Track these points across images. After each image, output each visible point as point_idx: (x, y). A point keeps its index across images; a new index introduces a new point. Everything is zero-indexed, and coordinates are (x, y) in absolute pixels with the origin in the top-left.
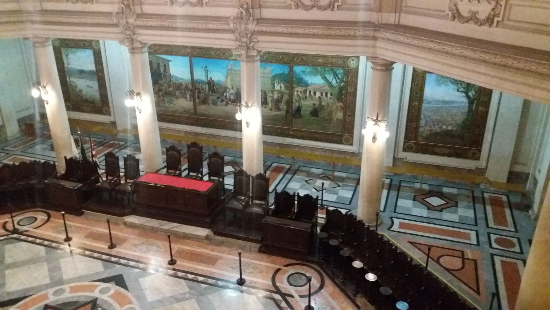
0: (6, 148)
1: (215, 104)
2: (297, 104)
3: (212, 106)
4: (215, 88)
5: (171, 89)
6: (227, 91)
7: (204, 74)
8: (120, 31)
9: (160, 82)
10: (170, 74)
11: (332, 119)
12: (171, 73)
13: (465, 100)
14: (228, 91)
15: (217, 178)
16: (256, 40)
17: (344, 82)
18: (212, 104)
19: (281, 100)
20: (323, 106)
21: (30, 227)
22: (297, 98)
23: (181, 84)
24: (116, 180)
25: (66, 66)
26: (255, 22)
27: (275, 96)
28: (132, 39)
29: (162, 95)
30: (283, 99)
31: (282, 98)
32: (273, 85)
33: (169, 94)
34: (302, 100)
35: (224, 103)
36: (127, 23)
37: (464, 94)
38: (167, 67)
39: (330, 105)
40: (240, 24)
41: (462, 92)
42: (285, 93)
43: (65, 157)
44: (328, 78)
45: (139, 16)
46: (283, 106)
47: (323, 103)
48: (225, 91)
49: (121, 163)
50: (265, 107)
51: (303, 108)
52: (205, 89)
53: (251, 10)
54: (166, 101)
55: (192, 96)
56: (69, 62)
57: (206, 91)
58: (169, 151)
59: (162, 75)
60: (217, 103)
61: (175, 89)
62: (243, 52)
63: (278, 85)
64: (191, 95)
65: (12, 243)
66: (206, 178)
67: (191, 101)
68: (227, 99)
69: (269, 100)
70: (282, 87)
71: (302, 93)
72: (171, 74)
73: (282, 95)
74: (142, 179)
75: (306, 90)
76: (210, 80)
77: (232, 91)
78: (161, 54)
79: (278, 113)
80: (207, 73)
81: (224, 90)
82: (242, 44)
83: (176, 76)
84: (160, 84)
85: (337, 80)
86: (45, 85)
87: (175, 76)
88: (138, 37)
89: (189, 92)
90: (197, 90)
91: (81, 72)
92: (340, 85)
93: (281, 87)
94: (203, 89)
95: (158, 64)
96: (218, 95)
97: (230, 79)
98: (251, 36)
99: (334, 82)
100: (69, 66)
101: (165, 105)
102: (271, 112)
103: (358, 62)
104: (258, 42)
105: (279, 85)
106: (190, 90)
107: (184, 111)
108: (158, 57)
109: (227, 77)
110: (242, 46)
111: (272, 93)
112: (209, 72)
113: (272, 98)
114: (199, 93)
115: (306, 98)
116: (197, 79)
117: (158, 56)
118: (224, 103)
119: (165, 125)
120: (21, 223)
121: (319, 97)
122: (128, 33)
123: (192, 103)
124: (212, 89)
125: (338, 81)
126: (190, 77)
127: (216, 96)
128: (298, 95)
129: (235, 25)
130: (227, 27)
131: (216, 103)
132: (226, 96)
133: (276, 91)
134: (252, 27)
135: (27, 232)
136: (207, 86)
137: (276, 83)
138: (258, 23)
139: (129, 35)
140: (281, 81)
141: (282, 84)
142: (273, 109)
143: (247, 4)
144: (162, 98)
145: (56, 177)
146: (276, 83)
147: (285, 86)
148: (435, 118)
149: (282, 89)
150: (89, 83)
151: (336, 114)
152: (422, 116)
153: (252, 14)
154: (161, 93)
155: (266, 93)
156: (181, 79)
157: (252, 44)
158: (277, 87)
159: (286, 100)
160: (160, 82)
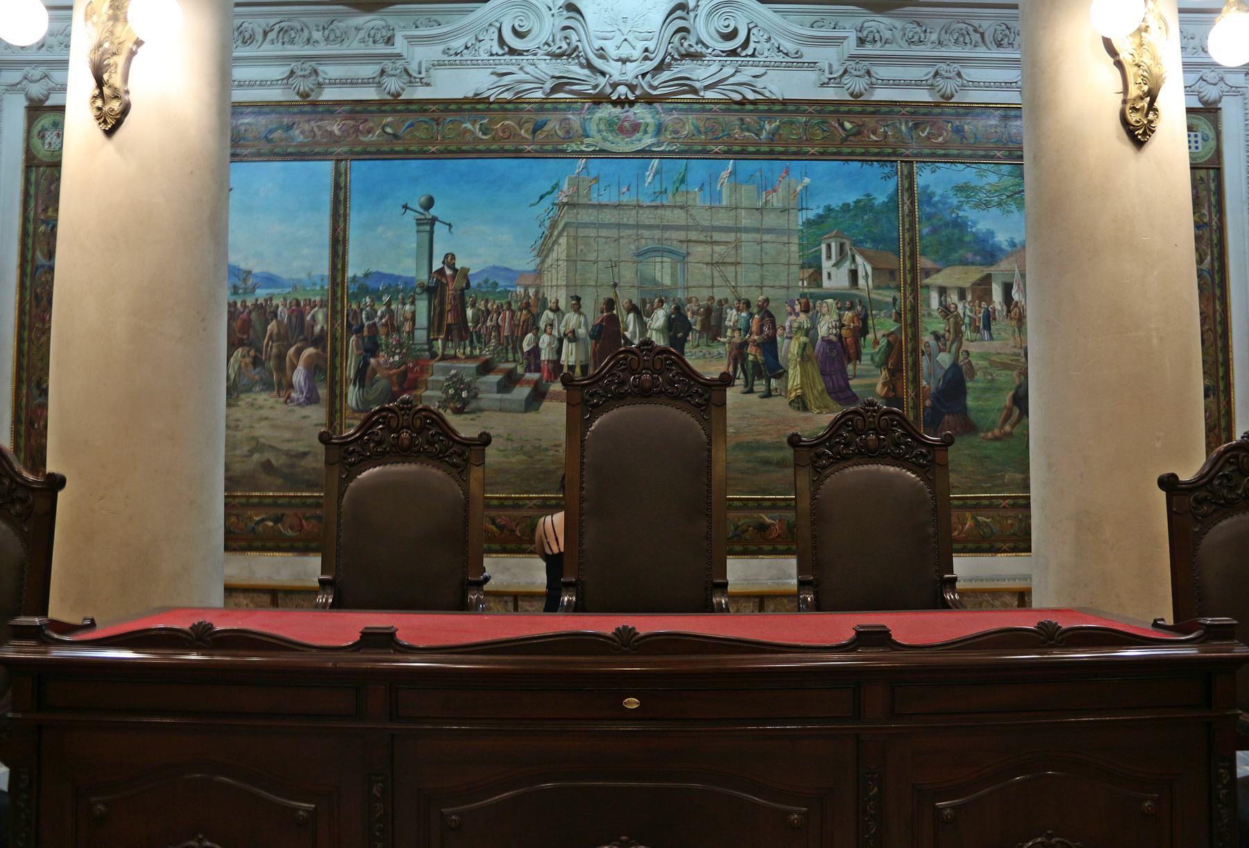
2: (945, 359)
4: (469, 312)
6: (542, 325)
7: (411, 240)
19: (857, 343)
22: (940, 326)
23: (266, 311)
27: (823, 330)
30: (870, 336)
31: (863, 331)
34: (968, 334)
35: (522, 392)
42: (880, 305)
48: (532, 325)
50: (768, 394)
51: (979, 375)
52: (407, 327)
57: (411, 333)
60: (475, 397)
64: (314, 369)
67: (312, 399)
68: (538, 369)
69: (790, 348)
70: (861, 273)
71: (969, 298)
73: (864, 320)
75: (987, 280)
76: (441, 271)
77: (572, 319)
80: (431, 233)
81: (522, 316)
93: (854, 274)
94: (392, 327)
96: (487, 353)
97: (563, 256)
102: (803, 415)
103: (1212, 135)
105: (847, 265)
106: (318, 341)
107: (267, 466)
109: (544, 251)
111: (806, 310)
113: (804, 339)
114: (372, 349)
115: (989, 318)
116: (366, 275)
118: (522, 392)
123: (317, 415)
126: (324, 268)
127: (471, 357)
128: (946, 311)
131: (465, 402)
132: (536, 351)
136: (422, 306)
137: (829, 257)
140: (855, 243)
141: (859, 259)
142: (810, 399)
146: (829, 257)
149: (861, 282)
155: (770, 315)
156: (270, 280)
158: (836, 279)
159: (883, 342)
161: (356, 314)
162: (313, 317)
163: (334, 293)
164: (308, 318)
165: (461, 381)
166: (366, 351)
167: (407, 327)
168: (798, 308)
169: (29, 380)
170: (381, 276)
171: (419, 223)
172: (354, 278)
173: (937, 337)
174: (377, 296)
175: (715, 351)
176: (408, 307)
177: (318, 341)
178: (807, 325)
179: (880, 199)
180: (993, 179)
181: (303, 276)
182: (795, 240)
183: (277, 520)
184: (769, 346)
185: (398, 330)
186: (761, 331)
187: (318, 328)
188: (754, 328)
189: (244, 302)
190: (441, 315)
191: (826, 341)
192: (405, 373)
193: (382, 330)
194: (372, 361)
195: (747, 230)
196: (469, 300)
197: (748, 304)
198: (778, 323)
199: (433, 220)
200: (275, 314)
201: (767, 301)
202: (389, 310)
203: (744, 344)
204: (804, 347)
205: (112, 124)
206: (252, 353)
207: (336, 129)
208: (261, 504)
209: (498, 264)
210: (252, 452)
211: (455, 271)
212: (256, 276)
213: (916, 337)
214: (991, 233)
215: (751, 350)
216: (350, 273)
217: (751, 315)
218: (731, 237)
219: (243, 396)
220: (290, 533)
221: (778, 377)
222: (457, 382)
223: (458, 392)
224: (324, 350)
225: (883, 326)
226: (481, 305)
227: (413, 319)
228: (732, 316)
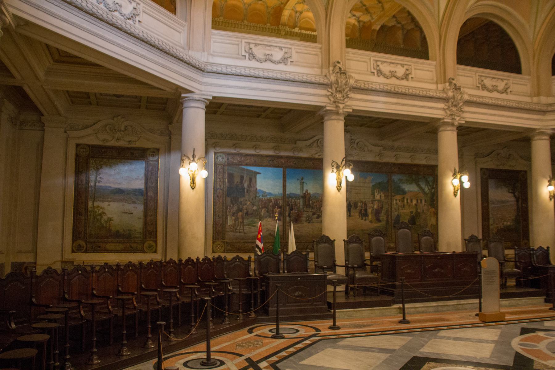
2: (396, 213)
3: (306, 224)
4: (311, 202)
5: (255, 208)
7: (299, 187)
9: (241, 200)
10: (257, 189)
11: (427, 225)
13: (513, 199)
17: (433, 188)
20: (419, 213)
22: (395, 207)
23: (269, 201)
25: (92, 184)
27: (375, 207)
30: (384, 209)
31: (382, 208)
32: (373, 194)
34: (400, 208)
37: (513, 194)
38: (253, 180)
39: (425, 212)
41: (511, 193)
44: (422, 186)
46: (383, 217)
47: (419, 210)
50: (365, 220)
52: (299, 205)
54: (245, 223)
56: (98, 179)
57: (299, 206)
60: (312, 220)
61: (261, 207)
63: (378, 194)
64: (280, 214)
69: (369, 211)
70: (382, 196)
73: (382, 205)
75: (404, 198)
76: (305, 193)
79: (379, 224)
80: (303, 185)
83: (264, 190)
84: (241, 203)
85: (429, 186)
87: (262, 191)
92: (431, 191)
94: (296, 205)
95: (242, 177)
96: (314, 211)
99: (426, 189)
100: (97, 184)
101: (244, 230)
102: (371, 224)
106: (281, 207)
108: (244, 170)
111: (372, 203)
112: (305, 185)
115: (404, 206)
116: (290, 193)
117: (243, 168)
121: (415, 204)
124: (307, 203)
125: (430, 188)
126: (281, 191)
127: (311, 211)
128: (397, 203)
131: (310, 221)
133: (377, 201)
136: (301, 201)
137: (376, 193)
141: (382, 193)
144: (240, 220)
147: (385, 196)
148: (499, 216)
149: (382, 198)
150: (129, 207)
151: (430, 220)
152: (491, 216)
154: (240, 213)
155: (366, 204)
156: (270, 194)
158: (377, 197)
161: (288, 202)
162: (279, 203)
163: (284, 197)
164: (278, 202)
165: (309, 216)
166: (291, 210)
167: (299, 205)
168: (371, 203)
169: (216, 215)
170: (293, 194)
171: (301, 183)
172: (288, 194)
173: (395, 209)
174: (292, 198)
175: (356, 211)
176: (299, 201)
177: (281, 207)
178: (372, 206)
179: (385, 181)
180: (405, 178)
181: (277, 193)
182: (370, 189)
185: (297, 205)
186: (364, 207)
187: (280, 205)
189: (265, 199)
190: (305, 202)
191: (376, 209)
193: (293, 206)
194: (292, 212)
195: (362, 187)
196: (311, 199)
197: (362, 202)
198: (368, 206)
199: (303, 182)
200: (271, 201)
202: (295, 201)
203: (361, 210)
204: (372, 210)
206: (267, 210)
207: (283, 161)
211: (308, 193)
212: (267, 193)
213: (391, 208)
214: (404, 189)
215: (363, 211)
216: (287, 193)
219: (265, 219)
222: (308, 217)
224: (282, 209)
225: (386, 207)
226: (313, 200)
227: (300, 203)
228: (359, 204)
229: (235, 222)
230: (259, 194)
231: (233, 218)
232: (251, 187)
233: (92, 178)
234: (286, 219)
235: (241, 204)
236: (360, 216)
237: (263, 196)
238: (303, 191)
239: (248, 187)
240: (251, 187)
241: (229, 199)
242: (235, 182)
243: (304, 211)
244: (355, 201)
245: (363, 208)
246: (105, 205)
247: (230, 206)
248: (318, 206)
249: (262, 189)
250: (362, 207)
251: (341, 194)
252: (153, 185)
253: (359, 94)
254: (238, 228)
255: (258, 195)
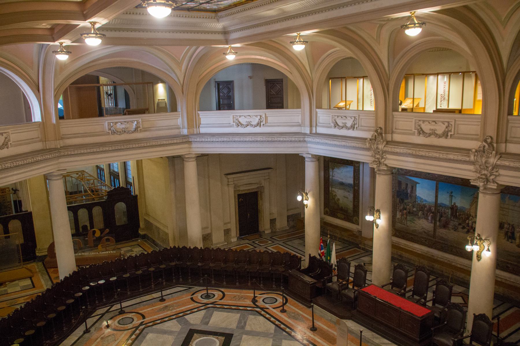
0: (273, 237)
1: (455, 229)
3: (452, 231)
4: (458, 214)
5: (415, 209)
6: (470, 219)
7: (448, 199)
8: (371, 155)
10: (416, 195)
12: (417, 194)
14: (471, 219)
15: (441, 307)
16: (497, 174)
18: (452, 229)
21: (270, 306)
23: (425, 206)
24: (345, 284)
25: (331, 177)
26: (498, 157)
28: (379, 162)
29: (406, 213)
33: (412, 213)
35: (466, 230)
36: (377, 148)
40: (482, 156)
43: (310, 255)
45: (388, 143)
48: (468, 218)
49: (352, 270)
50: (512, 243)
52: (447, 214)
53: (495, 145)
54: (408, 219)
55: (434, 218)
58: (396, 269)
59: (409, 195)
60: (457, 229)
62: (481, 184)
64: (432, 218)
65: (254, 315)
66: (430, 304)
67: (431, 223)
72: (417, 195)
74: (366, 290)
76: (453, 205)
78: (410, 176)
80: (452, 198)
81: (466, 216)
82: (482, 177)
86: (307, 192)
87: (420, 198)
88: (385, 160)
89: (431, 214)
90: (440, 213)
91: (342, 184)
94: (445, 214)
95: (407, 185)
96: (460, 222)
98: (493, 169)
100: (333, 178)
101: (407, 224)
104: (499, 175)
106: (433, 213)
107: (425, 232)
108: (408, 179)
110: (481, 178)
112: (453, 198)
114: (441, 216)
116: (441, 203)
118: (466, 230)
119: (403, 243)
120: (265, 301)
122: (378, 156)
123: (432, 225)
126: (434, 200)
129: (475, 157)
130: (468, 159)
132: (468, 224)
134: (493, 160)
135: (268, 310)
136: (450, 211)
138: (501, 157)
139: (378, 158)
143: (491, 138)
144: (405, 216)
145: (299, 270)
150: (346, 194)
153: (495, 149)
154: (405, 211)
156: (425, 201)
157: (492, 177)
160: (406, 201)
161: (439, 210)
162: (432, 209)
174: (443, 207)
181: (430, 201)
183: (425, 241)
184: (513, 233)
186: (511, 230)
187: (433, 211)
188: (510, 229)
192: (446, 222)
196: (458, 211)
197: (509, 224)
199: (452, 196)
200: (426, 207)
201: (513, 224)
203: (507, 232)
205: (377, 228)
208: (423, 238)
209: (463, 206)
210: (422, 229)
216: (438, 202)
217: (510, 226)
218: (507, 210)
220: (427, 243)
221: (514, 240)
223: (455, 227)
227: (448, 213)
228: (506, 226)
229: (402, 216)
230: (417, 199)
231: (401, 213)
232: (413, 193)
233: (331, 173)
234: (437, 223)
235: (406, 205)
236: (505, 238)
237: (420, 201)
238: (452, 203)
239: (411, 192)
240: (413, 193)
241: (398, 199)
242: (402, 188)
243: (451, 220)
244: (502, 221)
245: (510, 231)
246: (336, 190)
247: (399, 205)
248: (463, 219)
249: (420, 196)
250: (508, 229)
251: (378, 230)
252: (357, 182)
253: (392, 155)
254: (403, 221)
255: (417, 200)
